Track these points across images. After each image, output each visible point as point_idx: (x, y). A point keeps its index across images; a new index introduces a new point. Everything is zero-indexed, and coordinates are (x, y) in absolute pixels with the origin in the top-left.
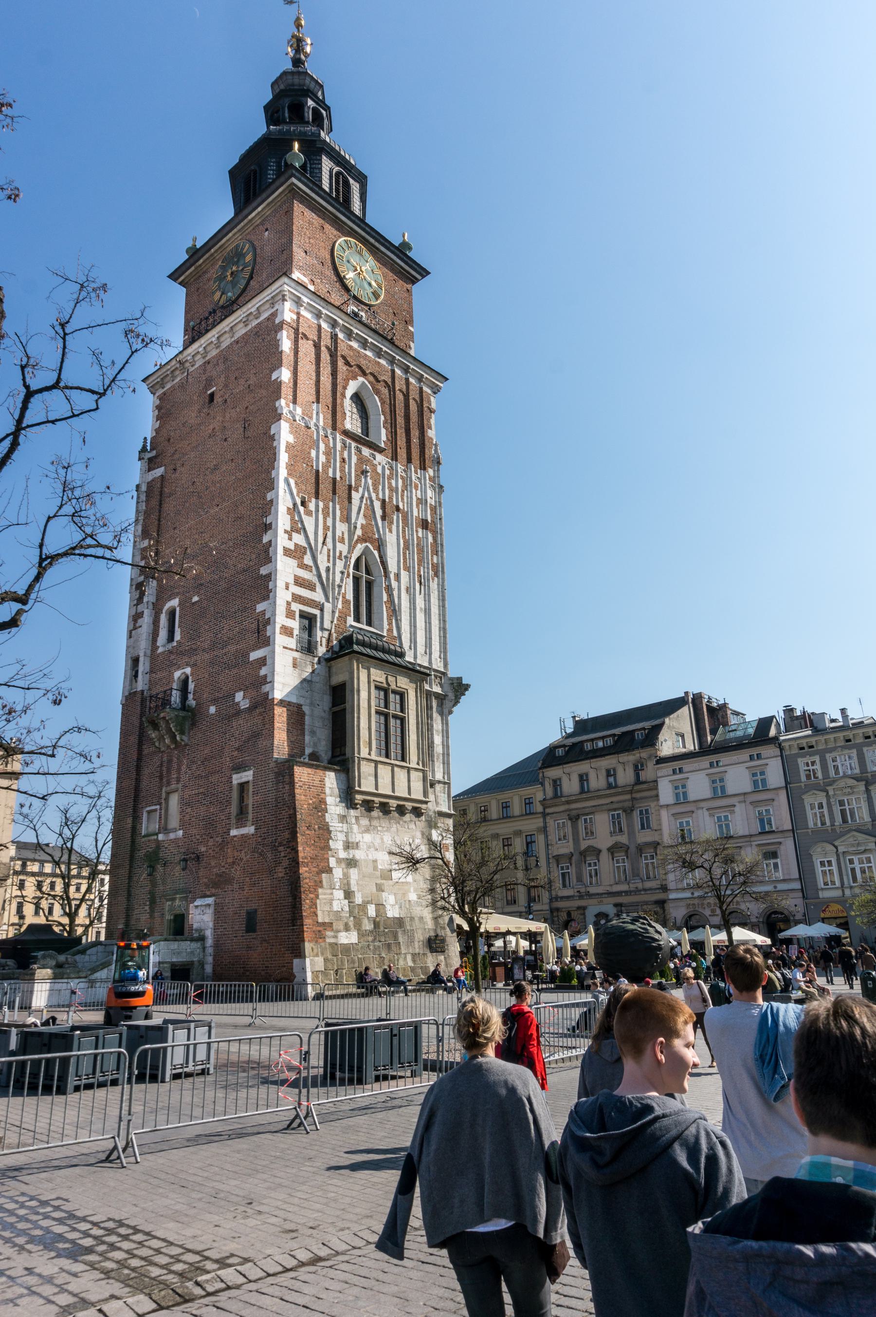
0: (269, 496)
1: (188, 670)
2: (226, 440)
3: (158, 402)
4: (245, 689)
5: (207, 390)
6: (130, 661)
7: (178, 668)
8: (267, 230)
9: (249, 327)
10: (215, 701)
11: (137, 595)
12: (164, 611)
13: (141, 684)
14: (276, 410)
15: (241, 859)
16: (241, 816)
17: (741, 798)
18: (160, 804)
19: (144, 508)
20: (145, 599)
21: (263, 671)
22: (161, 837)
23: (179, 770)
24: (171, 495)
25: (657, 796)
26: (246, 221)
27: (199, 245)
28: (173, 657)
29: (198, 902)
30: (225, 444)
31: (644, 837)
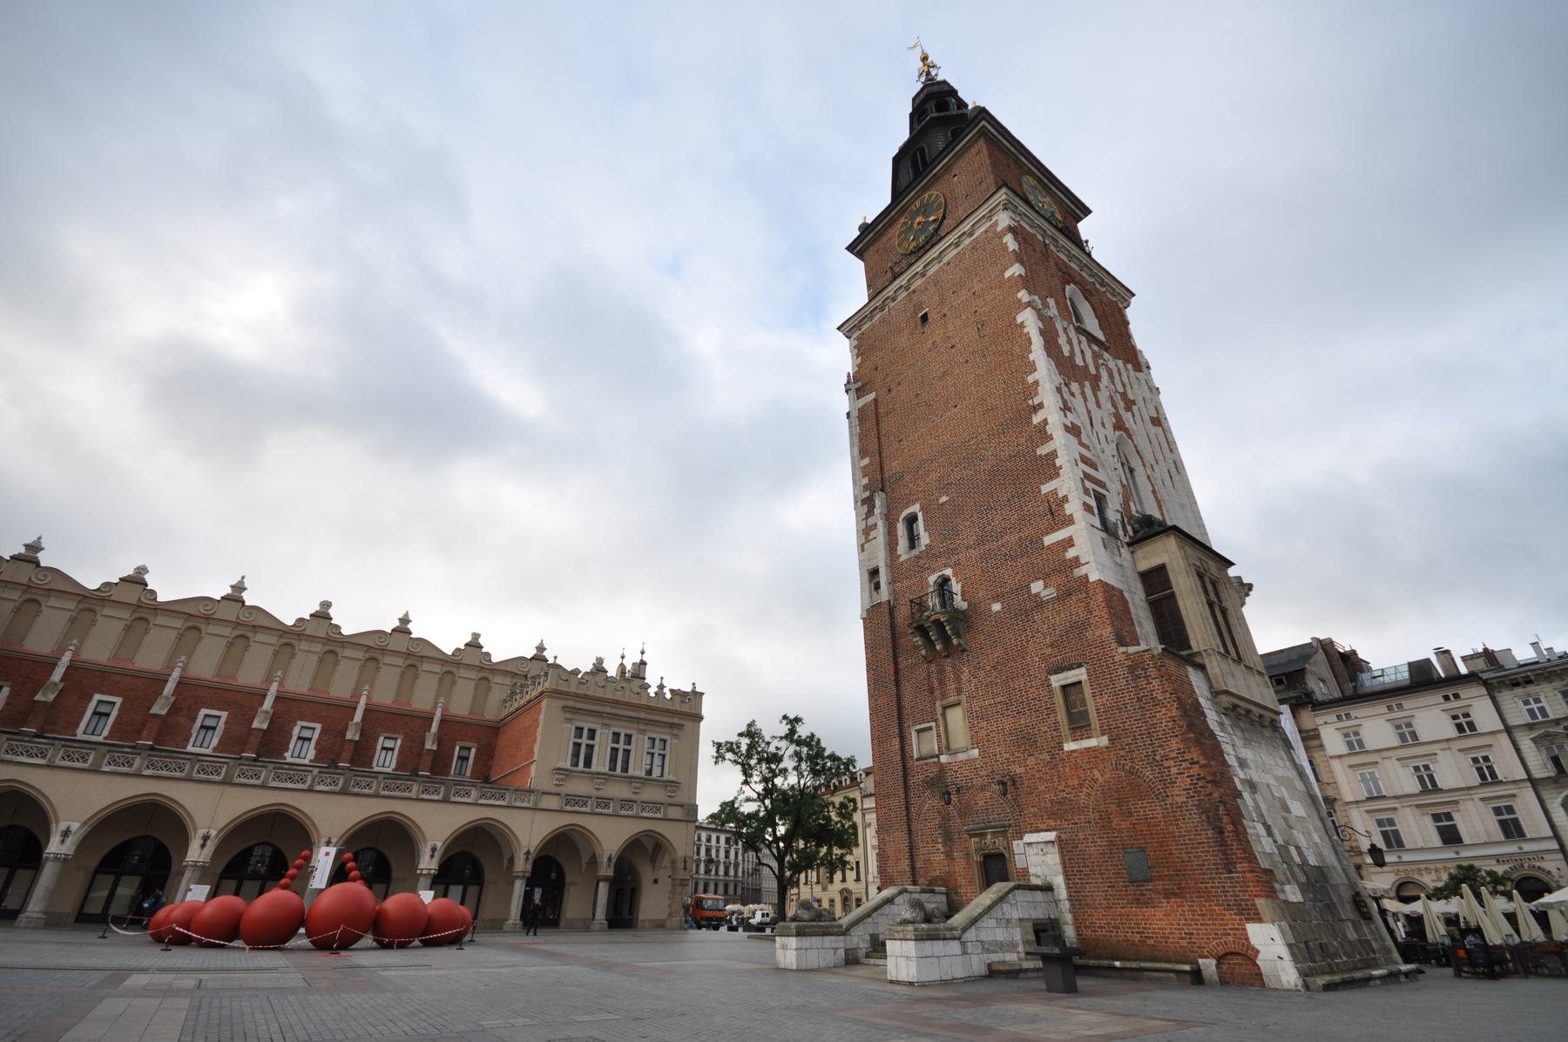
1: (948, 572)
4: (1046, 577)
6: (866, 576)
7: (934, 571)
10: (997, 598)
11: (865, 508)
13: (885, 594)
15: (1095, 781)
16: (1079, 725)
17: (1444, 745)
18: (936, 721)
20: (877, 511)
21: (1071, 553)
22: (944, 759)
23: (958, 680)
24: (887, 414)
25: (1321, 746)
27: (869, 221)
28: (921, 562)
29: (1028, 838)
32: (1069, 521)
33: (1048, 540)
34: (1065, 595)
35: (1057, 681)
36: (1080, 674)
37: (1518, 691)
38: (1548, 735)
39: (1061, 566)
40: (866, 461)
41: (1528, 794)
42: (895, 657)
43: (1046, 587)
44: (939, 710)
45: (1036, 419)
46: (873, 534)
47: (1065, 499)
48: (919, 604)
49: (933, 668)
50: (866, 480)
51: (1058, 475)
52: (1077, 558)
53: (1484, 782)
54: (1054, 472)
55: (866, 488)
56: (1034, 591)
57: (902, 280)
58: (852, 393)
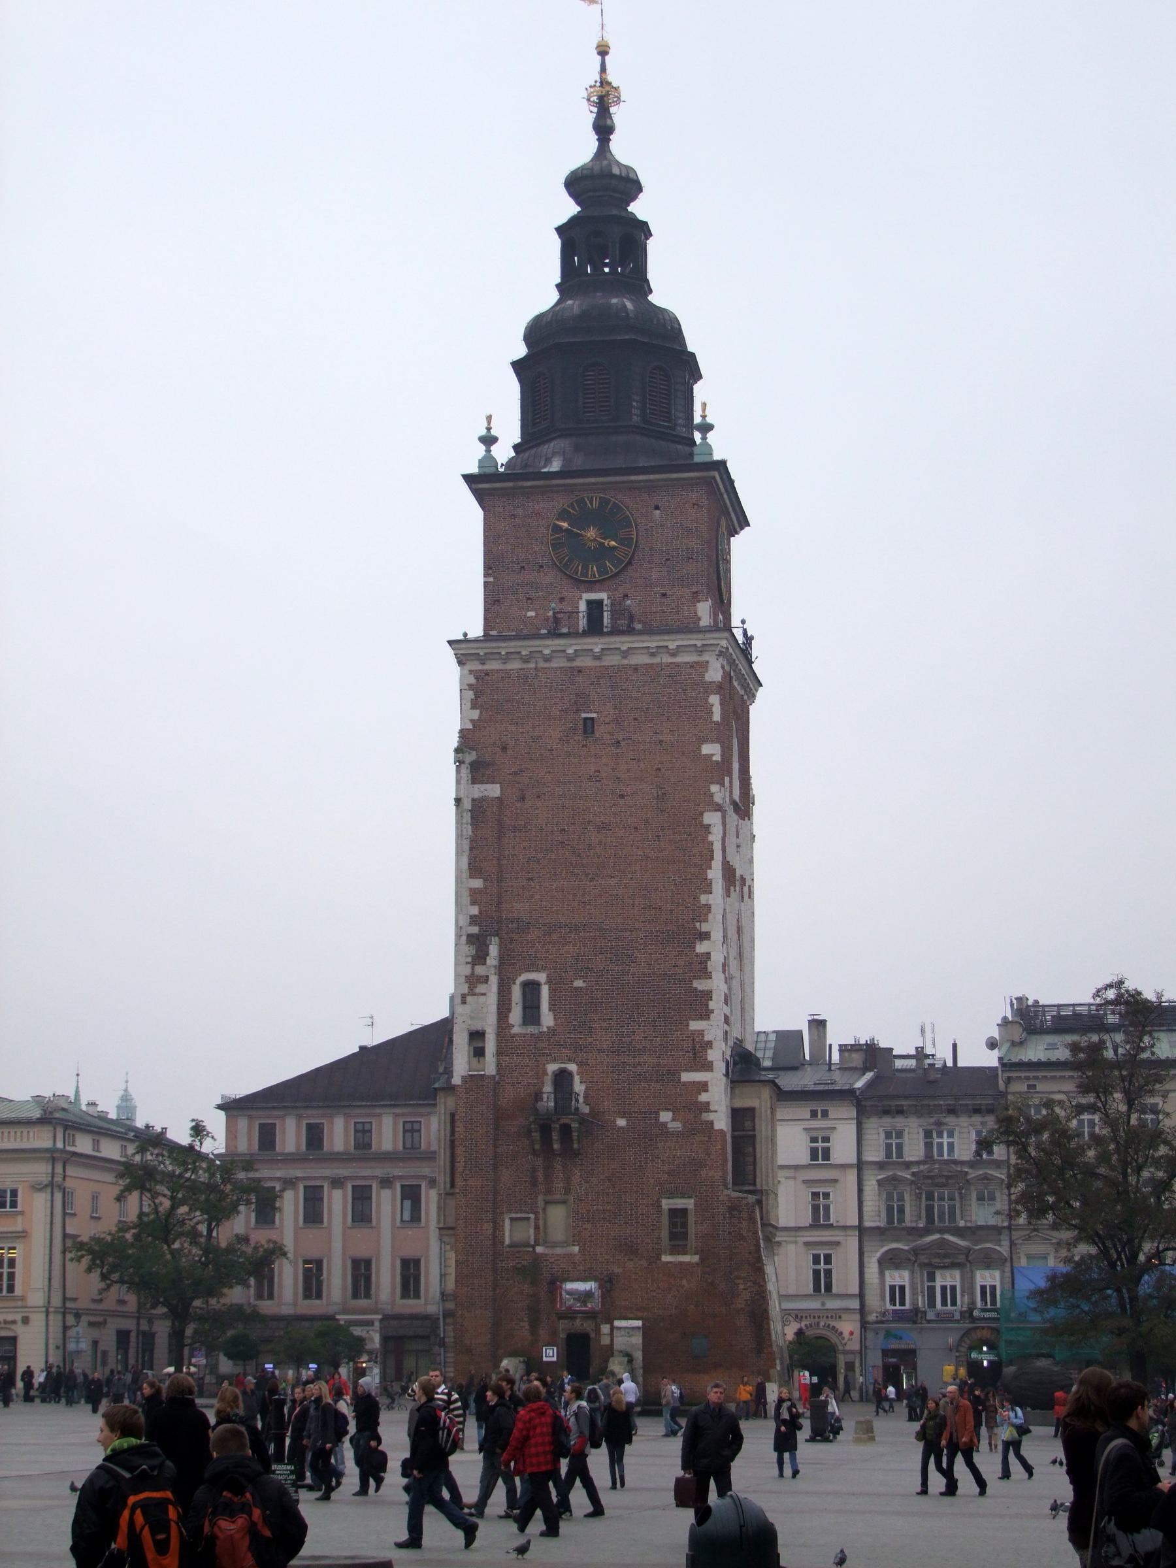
1: (573, 1067)
2: (622, 796)
3: (472, 680)
4: (675, 1111)
5: (578, 711)
7: (554, 1060)
8: (657, 508)
9: (657, 660)
12: (518, 982)
14: (711, 796)
17: (790, 1173)
18: (536, 1213)
19: (470, 833)
21: (703, 1097)
22: (539, 1249)
23: (567, 1180)
26: (625, 478)
29: (617, 1323)
30: (622, 802)
32: (708, 1067)
33: (686, 1077)
35: (666, 1204)
36: (689, 1203)
37: (887, 1121)
38: (894, 1179)
39: (691, 1105)
40: (478, 883)
41: (852, 1243)
42: (495, 1140)
43: (673, 1120)
44: (541, 1203)
45: (701, 948)
46: (480, 988)
47: (709, 1044)
48: (538, 1096)
49: (540, 1161)
50: (475, 910)
51: (708, 1018)
53: (816, 1225)
54: (705, 1014)
55: (473, 920)
57: (572, 646)
58: (465, 771)
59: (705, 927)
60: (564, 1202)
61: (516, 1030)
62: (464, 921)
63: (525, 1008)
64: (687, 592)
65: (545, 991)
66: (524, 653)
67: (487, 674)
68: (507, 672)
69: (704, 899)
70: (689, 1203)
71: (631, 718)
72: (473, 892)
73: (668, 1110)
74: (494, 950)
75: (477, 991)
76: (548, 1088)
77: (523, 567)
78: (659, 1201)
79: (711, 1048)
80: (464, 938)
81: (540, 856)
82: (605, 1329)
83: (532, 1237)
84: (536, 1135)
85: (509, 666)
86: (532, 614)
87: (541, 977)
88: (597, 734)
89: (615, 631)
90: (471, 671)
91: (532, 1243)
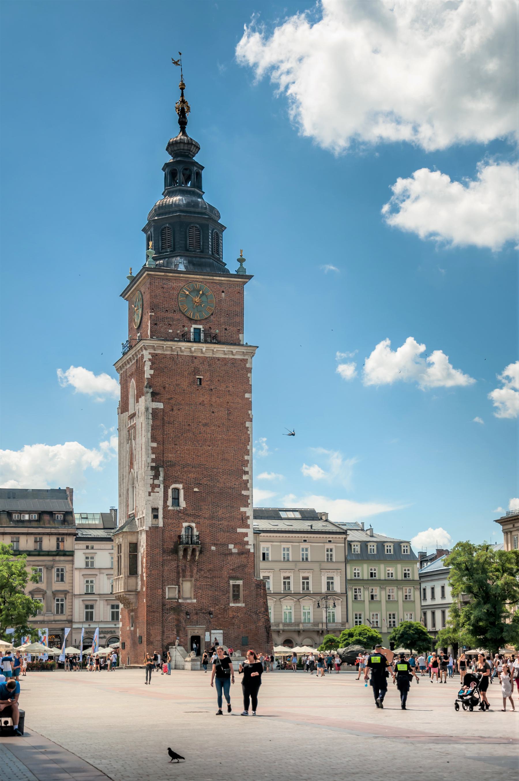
0: (246, 458)
1: (193, 525)
2: (213, 412)
3: (151, 357)
4: (235, 544)
5: (195, 375)
7: (186, 521)
8: (223, 292)
9: (227, 356)
10: (215, 545)
14: (249, 415)
15: (238, 616)
16: (236, 598)
20: (161, 478)
21: (246, 539)
22: (180, 601)
23: (191, 572)
26: (211, 278)
28: (180, 515)
29: (213, 631)
30: (213, 415)
31: (58, 586)
32: (248, 527)
33: (239, 530)
34: (241, 553)
36: (240, 582)
39: (241, 542)
40: (155, 445)
43: (234, 548)
45: (245, 477)
46: (157, 489)
50: (154, 456)
52: (248, 542)
54: (247, 505)
55: (153, 460)
56: (229, 548)
59: (246, 469)
60: (191, 581)
61: (170, 508)
62: (149, 460)
63: (173, 499)
64: (235, 329)
65: (182, 492)
66: (173, 348)
67: (157, 355)
68: (166, 355)
69: (246, 458)
70: (240, 582)
71: (217, 380)
72: (153, 448)
73: (232, 544)
74: (162, 474)
75: (155, 491)
76: (183, 533)
77: (167, 310)
78: (228, 581)
79: (249, 519)
80: (150, 468)
81: (180, 435)
82: (208, 634)
83: (177, 596)
84: (181, 553)
85: (166, 353)
86: (170, 331)
87: (180, 486)
88: (203, 385)
89: (206, 342)
90: (150, 353)
91: (177, 596)
